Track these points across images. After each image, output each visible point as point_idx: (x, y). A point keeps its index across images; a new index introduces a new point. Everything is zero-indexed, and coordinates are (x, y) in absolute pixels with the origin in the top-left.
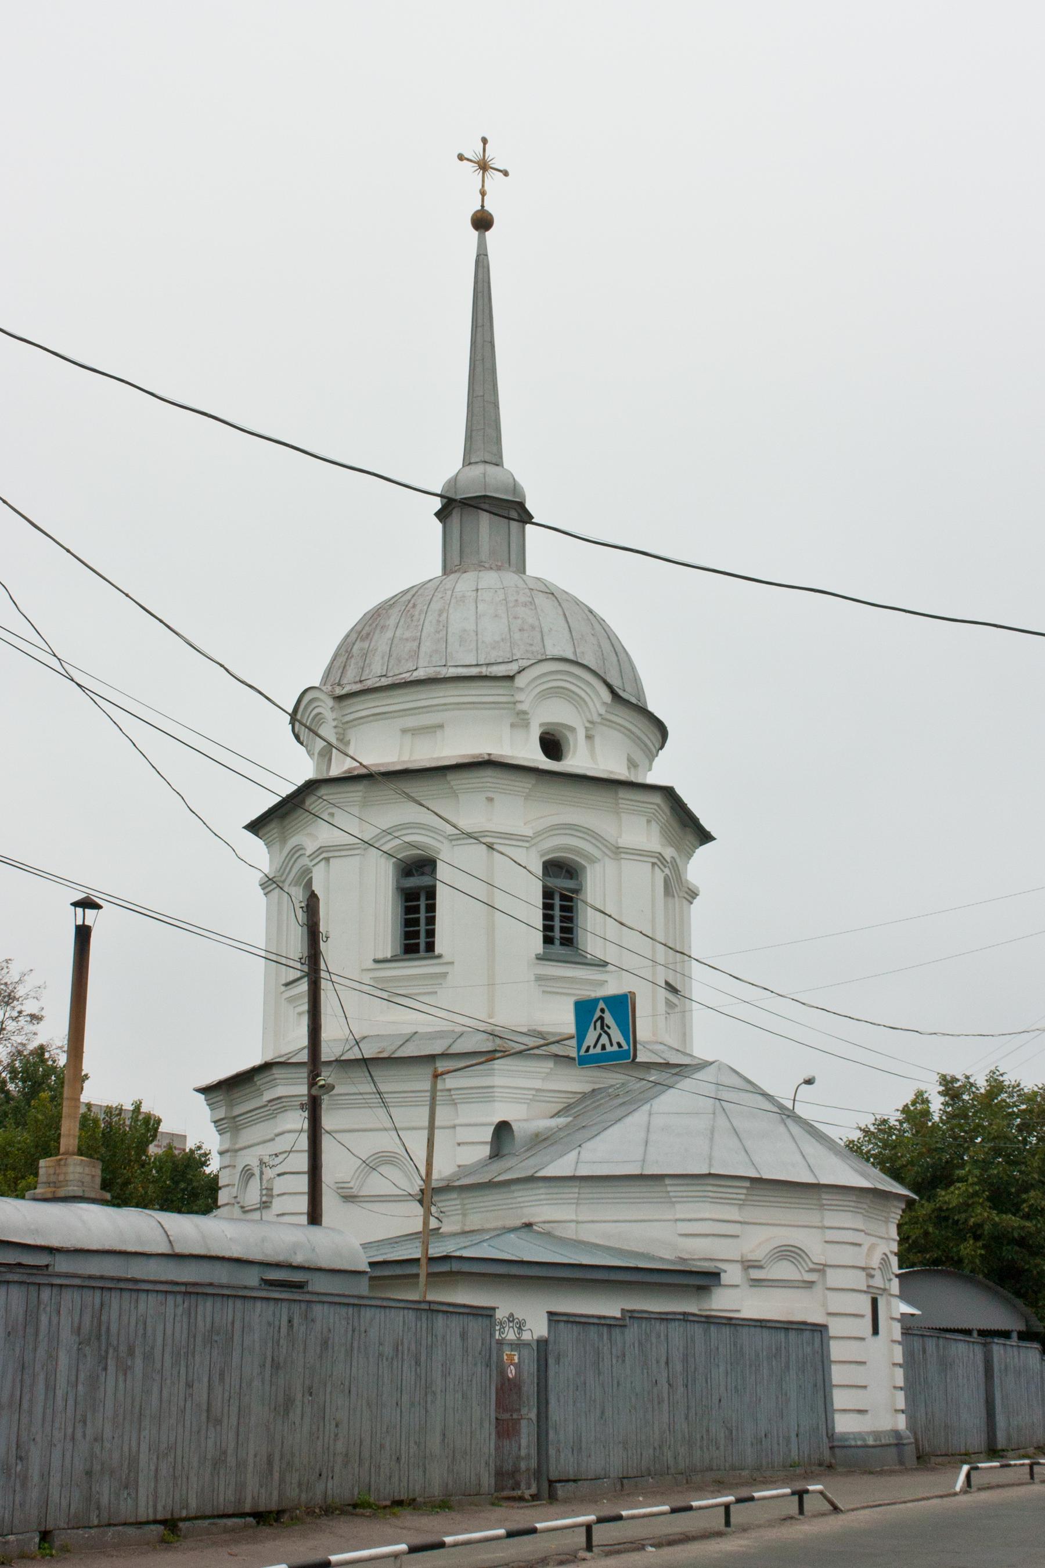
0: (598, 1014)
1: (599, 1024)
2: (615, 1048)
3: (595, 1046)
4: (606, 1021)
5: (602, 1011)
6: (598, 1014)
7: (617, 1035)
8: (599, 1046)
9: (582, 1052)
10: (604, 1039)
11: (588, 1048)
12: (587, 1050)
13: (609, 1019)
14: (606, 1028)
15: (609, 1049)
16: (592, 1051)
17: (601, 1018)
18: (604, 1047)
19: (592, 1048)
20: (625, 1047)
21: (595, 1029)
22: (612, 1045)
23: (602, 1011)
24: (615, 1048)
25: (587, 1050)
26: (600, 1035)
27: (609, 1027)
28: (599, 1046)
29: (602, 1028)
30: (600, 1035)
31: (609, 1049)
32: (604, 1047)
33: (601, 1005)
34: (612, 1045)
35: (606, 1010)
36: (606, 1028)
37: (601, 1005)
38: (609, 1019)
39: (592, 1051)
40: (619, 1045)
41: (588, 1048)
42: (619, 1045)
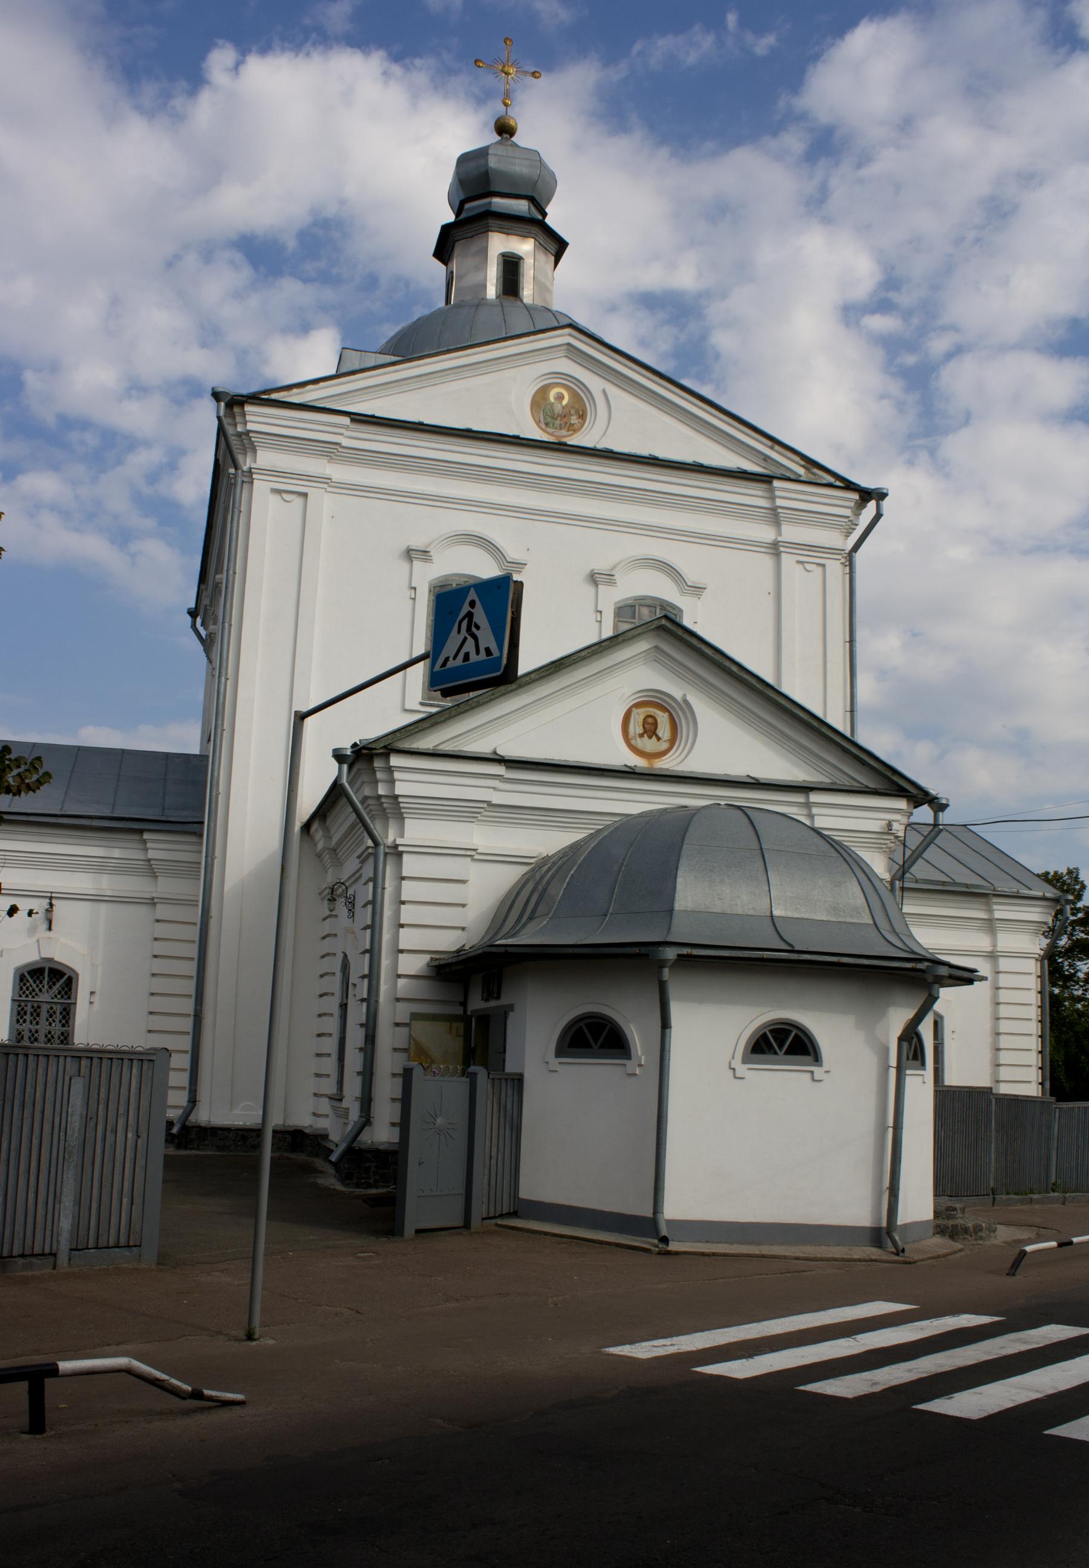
0: (466, 608)
1: (465, 624)
3: (455, 658)
4: (476, 619)
6: (466, 608)
7: (486, 638)
8: (461, 656)
9: (437, 668)
10: (470, 643)
11: (447, 659)
13: (480, 616)
14: (474, 629)
15: (474, 658)
16: (451, 664)
17: (470, 615)
18: (467, 657)
19: (451, 659)
21: (459, 632)
22: (478, 652)
23: (472, 604)
24: (483, 656)
25: (444, 664)
26: (465, 639)
27: (478, 627)
28: (461, 656)
29: (469, 630)
30: (465, 639)
31: (474, 658)
33: (472, 595)
34: (478, 652)
35: (478, 604)
36: (474, 629)
37: (472, 595)
38: (480, 616)
39: (451, 664)
41: (447, 659)
42: (488, 651)
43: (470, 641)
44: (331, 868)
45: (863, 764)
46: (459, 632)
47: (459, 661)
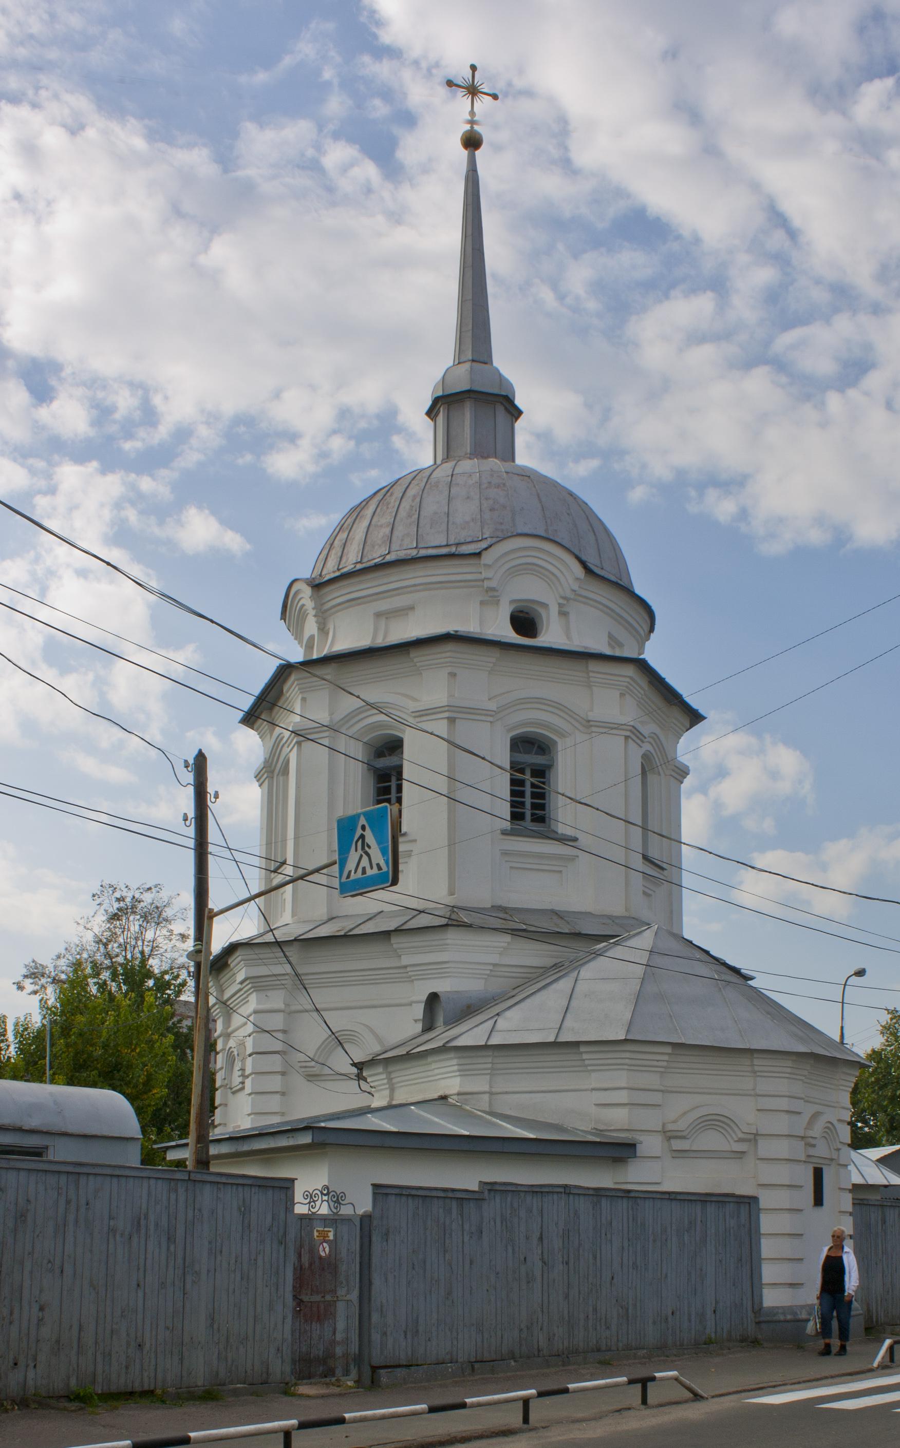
2: (375, 871)
3: (355, 872)
5: (363, 828)
6: (359, 832)
8: (360, 870)
9: (344, 880)
10: (365, 860)
12: (348, 877)
14: (367, 848)
15: (369, 872)
16: (353, 876)
17: (362, 837)
18: (364, 870)
19: (353, 872)
20: (385, 869)
21: (356, 850)
22: (372, 868)
23: (363, 828)
24: (375, 871)
25: (348, 877)
26: (361, 856)
27: (369, 847)
28: (360, 870)
29: (363, 848)
30: (361, 856)
31: (369, 872)
32: (364, 870)
33: (362, 821)
34: (372, 868)
35: (367, 828)
36: (367, 848)
37: (362, 821)
39: (353, 876)
40: (379, 868)
42: (379, 868)
43: (365, 858)
44: (244, 969)
46: (356, 850)
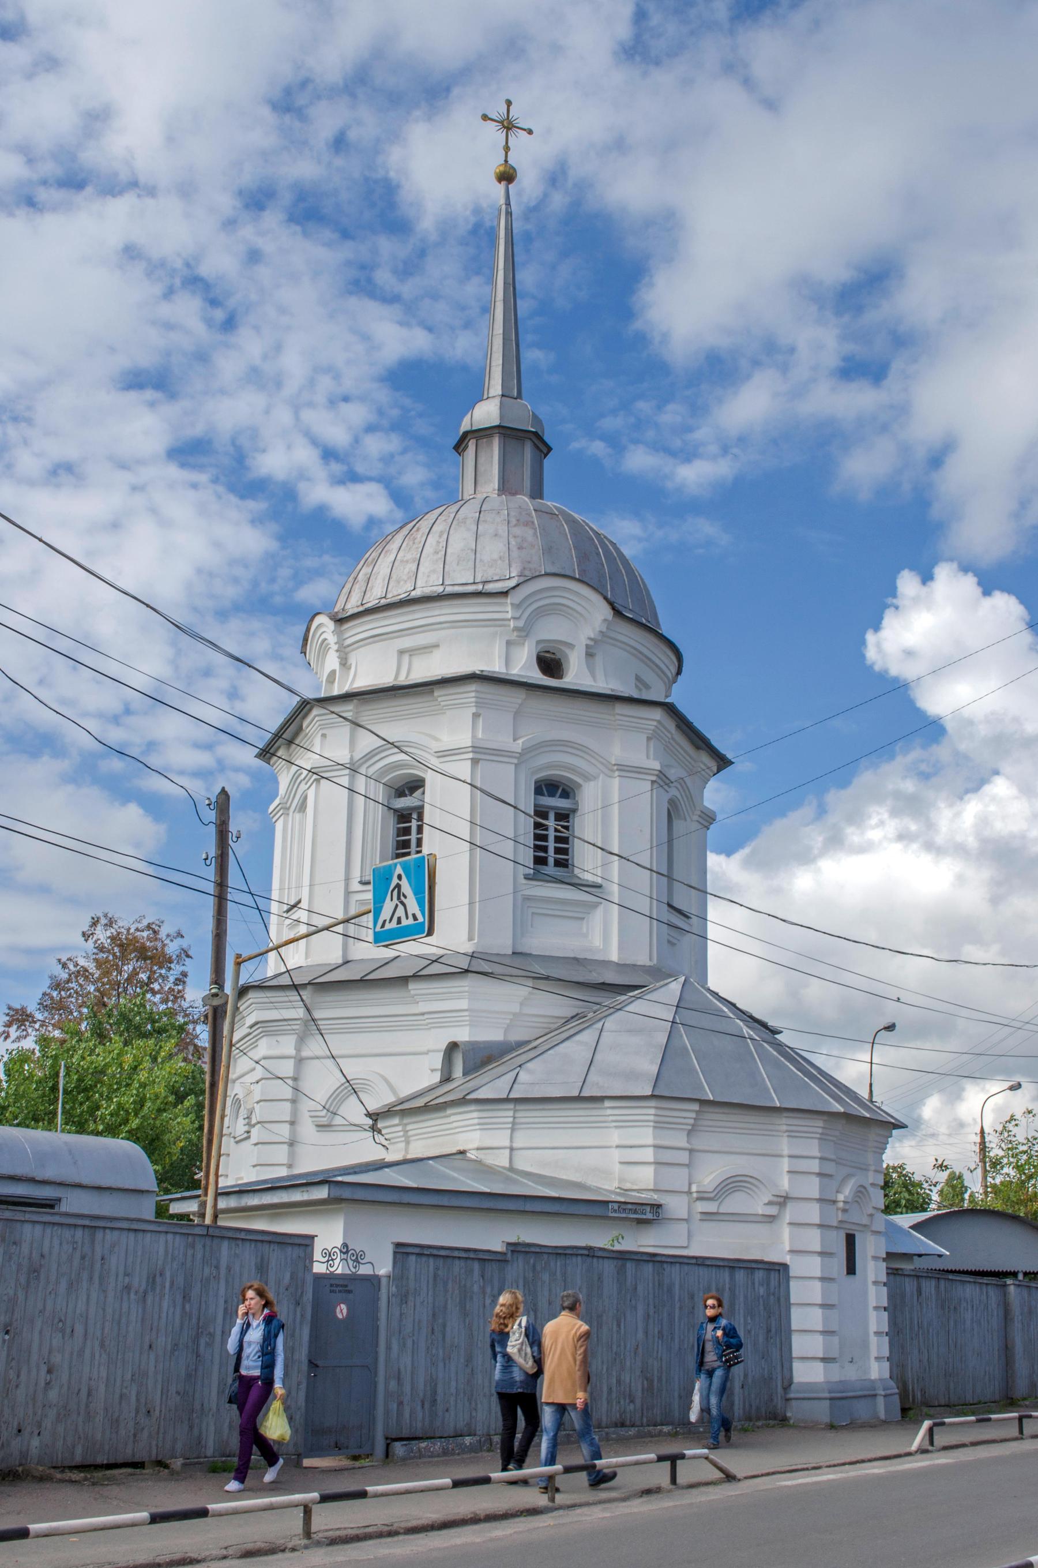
1: (395, 892)
2: (411, 921)
4: (403, 890)
5: (400, 877)
6: (395, 881)
8: (395, 920)
9: (378, 929)
10: (401, 909)
11: (385, 921)
12: (383, 926)
15: (405, 922)
16: (388, 926)
17: (398, 886)
18: (399, 921)
21: (392, 900)
22: (407, 918)
23: (400, 877)
24: (411, 921)
25: (383, 926)
26: (397, 905)
27: (405, 897)
28: (395, 920)
29: (399, 898)
30: (397, 905)
31: (405, 922)
32: (399, 921)
34: (407, 918)
35: (404, 877)
36: (402, 898)
38: (406, 888)
39: (388, 926)
40: (415, 918)
41: (385, 921)
43: (401, 908)
45: (603, 984)
46: (392, 900)
47: (394, 924)
